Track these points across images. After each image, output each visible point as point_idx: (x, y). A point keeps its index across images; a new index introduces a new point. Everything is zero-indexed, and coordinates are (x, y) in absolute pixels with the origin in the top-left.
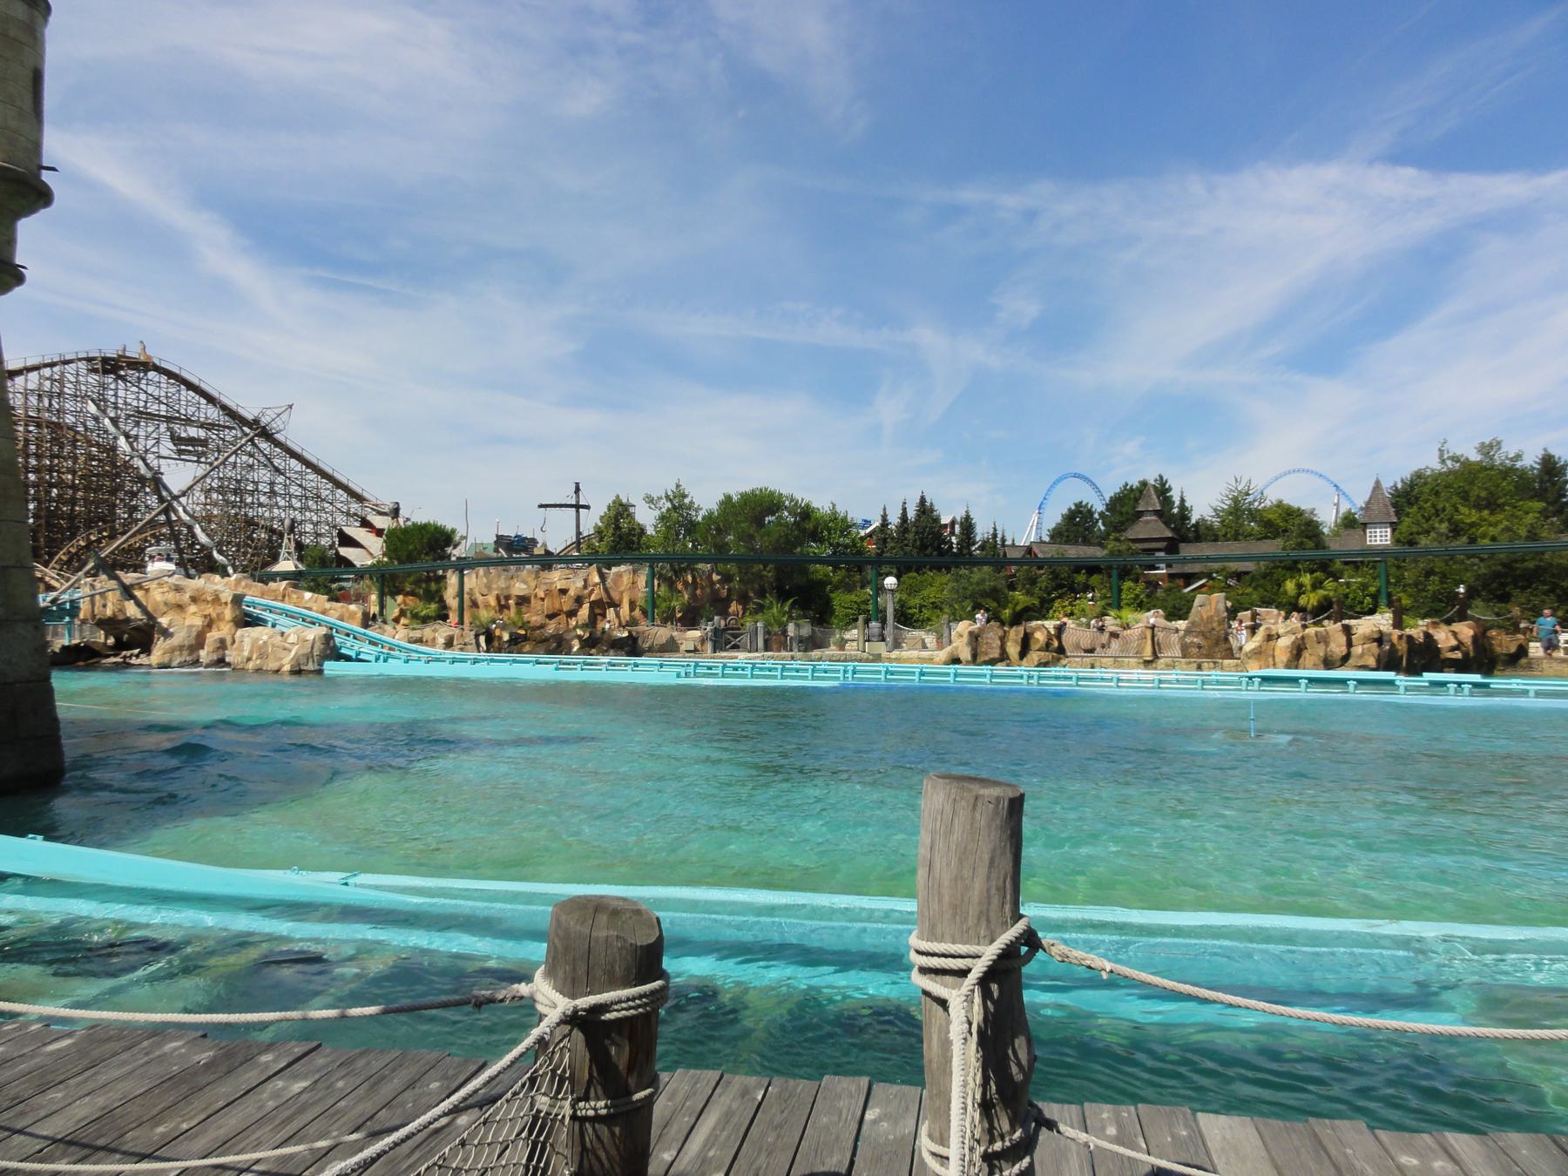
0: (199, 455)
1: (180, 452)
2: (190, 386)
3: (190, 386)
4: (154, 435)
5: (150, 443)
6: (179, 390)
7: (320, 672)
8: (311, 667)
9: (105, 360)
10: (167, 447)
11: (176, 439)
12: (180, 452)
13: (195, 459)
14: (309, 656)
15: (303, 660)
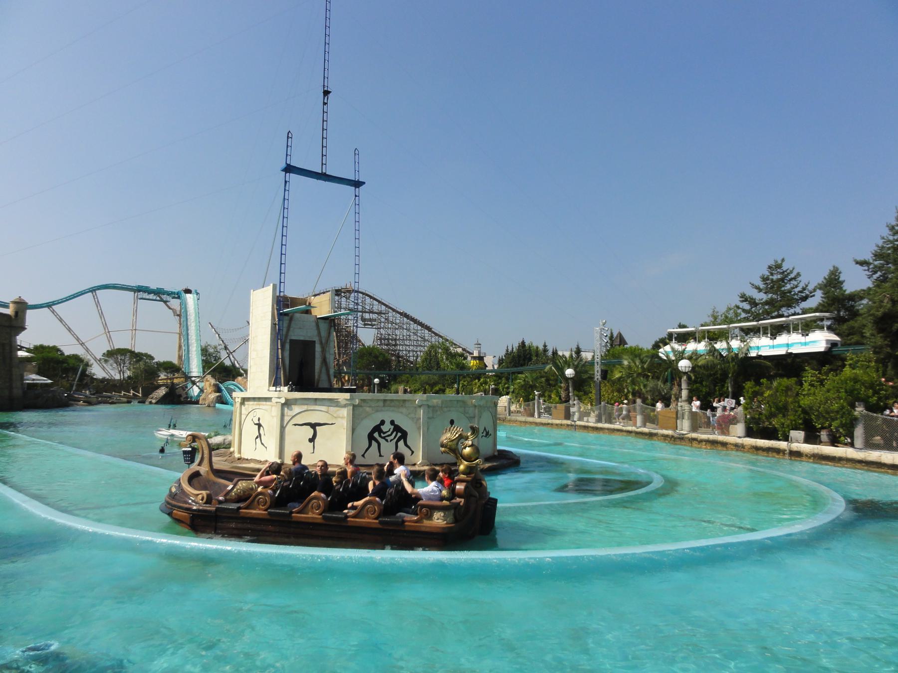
0: (372, 325)
1: (365, 325)
2: (371, 297)
3: (371, 297)
4: (356, 319)
5: (355, 321)
6: (365, 300)
7: (215, 406)
8: (212, 405)
9: (337, 291)
10: (360, 323)
11: (363, 320)
12: (365, 325)
13: (371, 327)
14: (212, 402)
15: (210, 403)
